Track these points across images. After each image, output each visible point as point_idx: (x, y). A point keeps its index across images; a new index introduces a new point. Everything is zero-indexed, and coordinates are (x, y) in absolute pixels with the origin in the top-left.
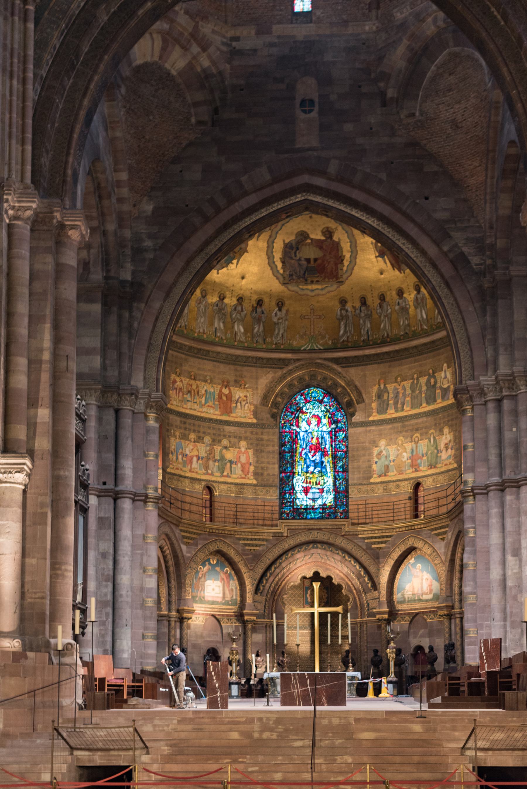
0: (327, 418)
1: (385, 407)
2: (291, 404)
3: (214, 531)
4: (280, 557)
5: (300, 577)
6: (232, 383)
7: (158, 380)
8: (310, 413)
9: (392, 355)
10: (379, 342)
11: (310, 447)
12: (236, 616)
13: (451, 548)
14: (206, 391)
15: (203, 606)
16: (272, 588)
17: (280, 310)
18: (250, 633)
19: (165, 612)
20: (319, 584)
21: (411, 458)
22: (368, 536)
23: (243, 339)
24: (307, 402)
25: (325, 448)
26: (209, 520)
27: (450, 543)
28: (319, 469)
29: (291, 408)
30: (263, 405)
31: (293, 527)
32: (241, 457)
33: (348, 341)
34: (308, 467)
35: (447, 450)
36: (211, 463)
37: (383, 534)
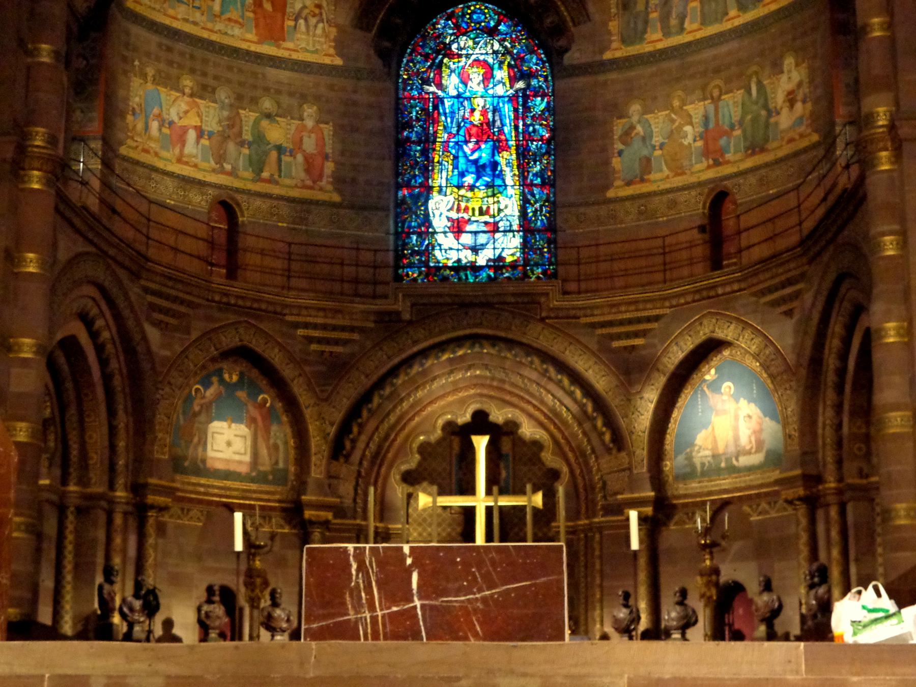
0: (505, 67)
1: (640, 26)
2: (424, 38)
4: (393, 372)
5: (440, 422)
11: (468, 131)
12: (284, 510)
13: (813, 330)
19: (98, 488)
21: (704, 136)
22: (602, 319)
24: (460, 32)
25: (501, 131)
27: (809, 318)
28: (488, 179)
29: (423, 47)
30: (361, 28)
32: (305, 139)
34: (462, 175)
37: (639, 314)
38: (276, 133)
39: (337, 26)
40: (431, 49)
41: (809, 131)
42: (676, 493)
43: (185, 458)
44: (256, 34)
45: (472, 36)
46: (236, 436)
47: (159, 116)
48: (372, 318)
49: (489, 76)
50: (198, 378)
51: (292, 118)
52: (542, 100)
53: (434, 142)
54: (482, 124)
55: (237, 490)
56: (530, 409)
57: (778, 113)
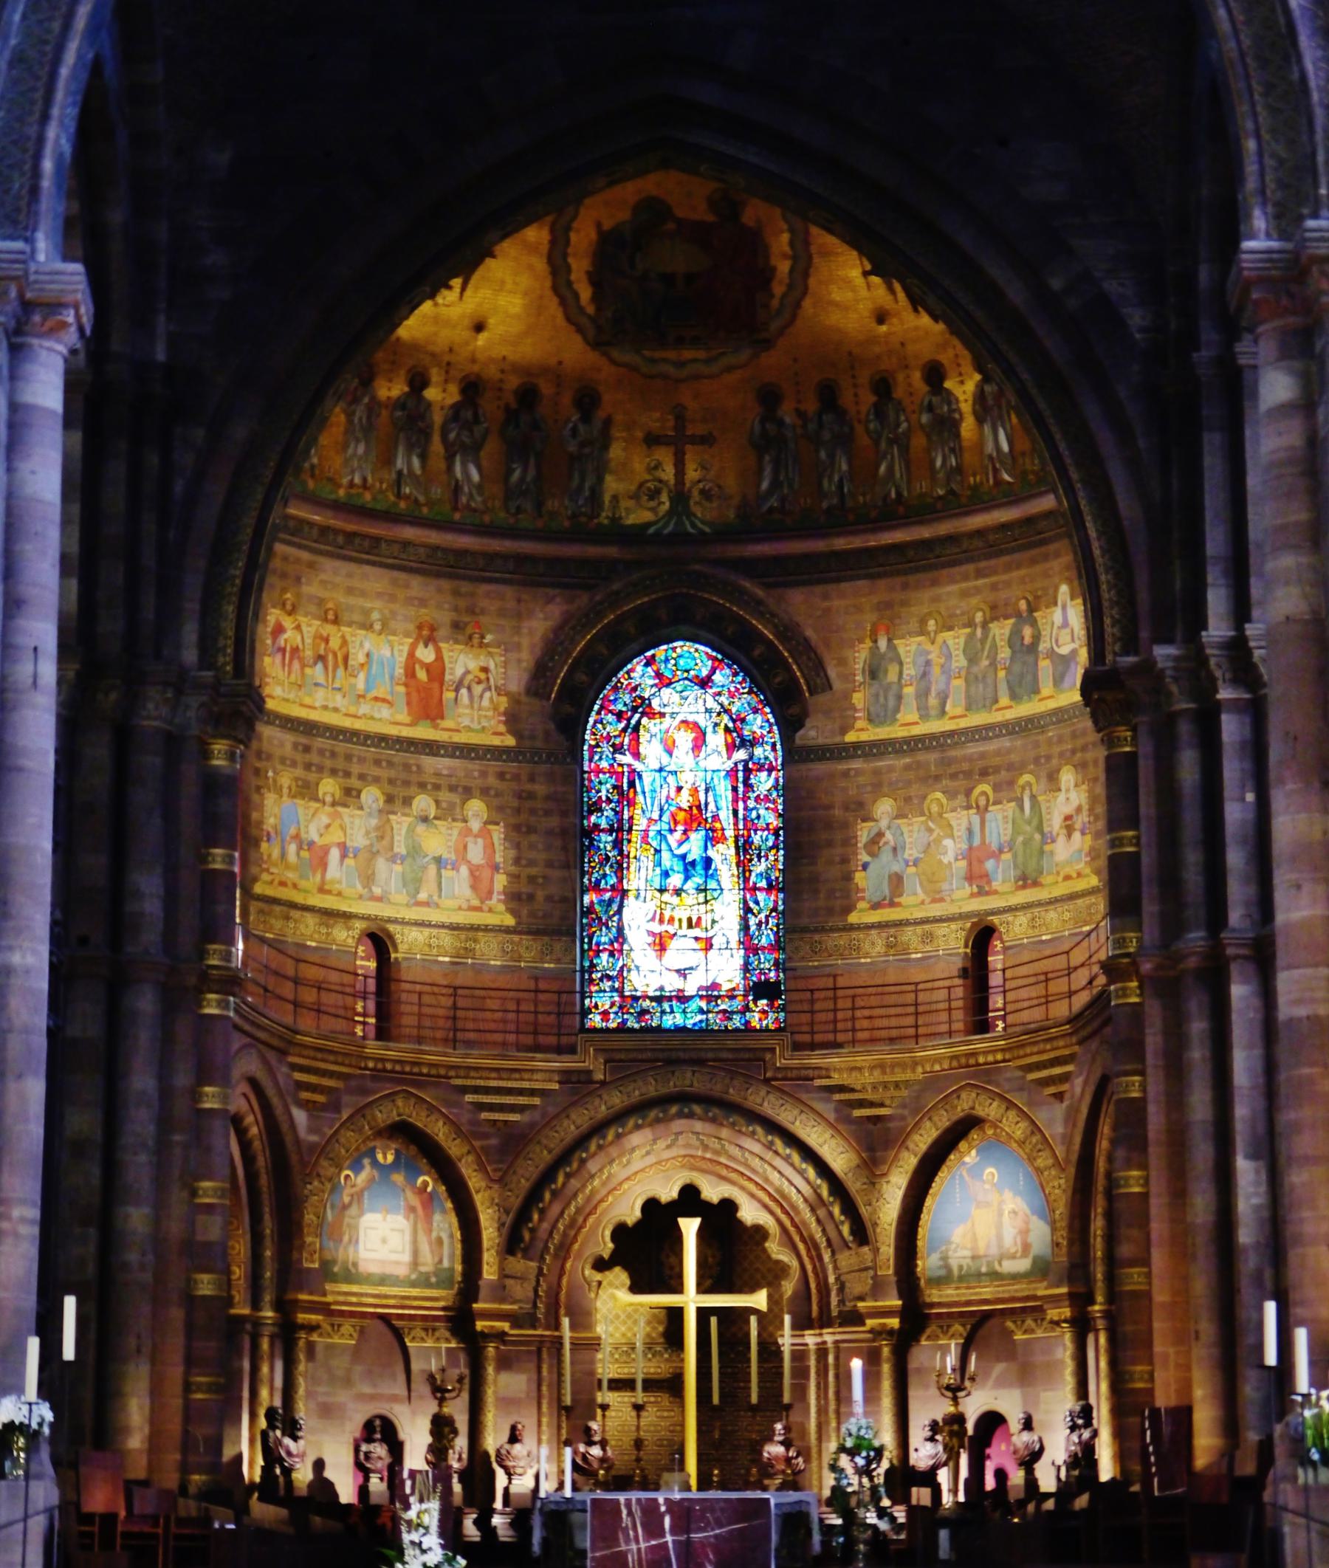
0: (721, 730)
1: (891, 703)
3: (389, 1066)
4: (581, 1142)
6: (442, 632)
8: (673, 715)
9: (911, 553)
10: (873, 514)
11: (673, 816)
12: (448, 1319)
14: (368, 655)
16: (557, 1237)
17: (586, 417)
18: (490, 1370)
25: (716, 818)
26: (372, 1033)
31: (623, 1056)
32: (470, 846)
34: (666, 874)
35: (1069, 836)
36: (381, 864)
39: (507, 694)
40: (625, 704)
41: (1088, 871)
42: (928, 1300)
43: (334, 1262)
44: (409, 714)
45: (679, 689)
46: (393, 1230)
47: (297, 837)
48: (557, 1078)
49: (700, 742)
51: (454, 820)
52: (769, 775)
53: (630, 831)
54: (691, 808)
55: (395, 1297)
56: (751, 1187)
57: (1053, 841)
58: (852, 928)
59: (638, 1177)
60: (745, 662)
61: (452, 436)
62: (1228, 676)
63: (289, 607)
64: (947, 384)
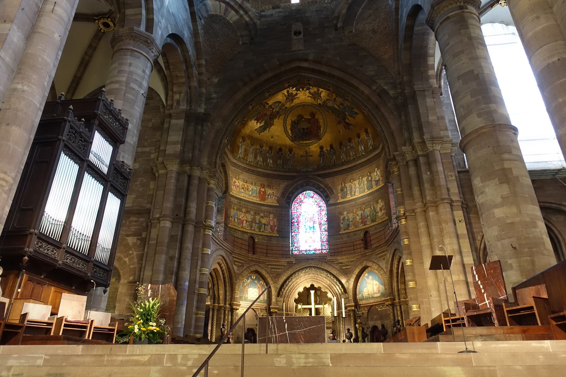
0: (316, 205)
1: (345, 195)
3: (254, 259)
4: (291, 275)
6: (266, 186)
7: (216, 163)
15: (247, 302)
17: (290, 153)
20: (314, 291)
23: (272, 166)
27: (389, 260)
33: (325, 166)
35: (381, 211)
36: (254, 224)
38: (264, 221)
47: (237, 218)
50: (246, 278)
57: (378, 213)
58: (341, 234)
59: (303, 282)
60: (319, 192)
61: (267, 155)
62: (420, 149)
63: (237, 179)
64: (352, 141)
